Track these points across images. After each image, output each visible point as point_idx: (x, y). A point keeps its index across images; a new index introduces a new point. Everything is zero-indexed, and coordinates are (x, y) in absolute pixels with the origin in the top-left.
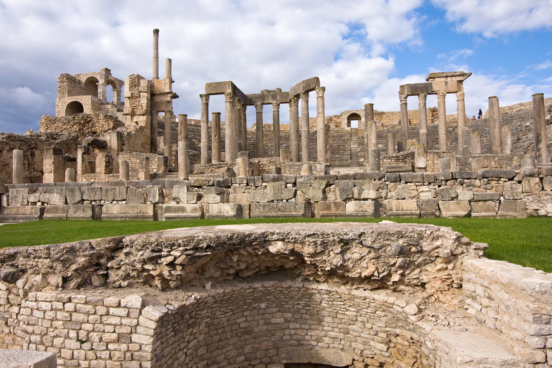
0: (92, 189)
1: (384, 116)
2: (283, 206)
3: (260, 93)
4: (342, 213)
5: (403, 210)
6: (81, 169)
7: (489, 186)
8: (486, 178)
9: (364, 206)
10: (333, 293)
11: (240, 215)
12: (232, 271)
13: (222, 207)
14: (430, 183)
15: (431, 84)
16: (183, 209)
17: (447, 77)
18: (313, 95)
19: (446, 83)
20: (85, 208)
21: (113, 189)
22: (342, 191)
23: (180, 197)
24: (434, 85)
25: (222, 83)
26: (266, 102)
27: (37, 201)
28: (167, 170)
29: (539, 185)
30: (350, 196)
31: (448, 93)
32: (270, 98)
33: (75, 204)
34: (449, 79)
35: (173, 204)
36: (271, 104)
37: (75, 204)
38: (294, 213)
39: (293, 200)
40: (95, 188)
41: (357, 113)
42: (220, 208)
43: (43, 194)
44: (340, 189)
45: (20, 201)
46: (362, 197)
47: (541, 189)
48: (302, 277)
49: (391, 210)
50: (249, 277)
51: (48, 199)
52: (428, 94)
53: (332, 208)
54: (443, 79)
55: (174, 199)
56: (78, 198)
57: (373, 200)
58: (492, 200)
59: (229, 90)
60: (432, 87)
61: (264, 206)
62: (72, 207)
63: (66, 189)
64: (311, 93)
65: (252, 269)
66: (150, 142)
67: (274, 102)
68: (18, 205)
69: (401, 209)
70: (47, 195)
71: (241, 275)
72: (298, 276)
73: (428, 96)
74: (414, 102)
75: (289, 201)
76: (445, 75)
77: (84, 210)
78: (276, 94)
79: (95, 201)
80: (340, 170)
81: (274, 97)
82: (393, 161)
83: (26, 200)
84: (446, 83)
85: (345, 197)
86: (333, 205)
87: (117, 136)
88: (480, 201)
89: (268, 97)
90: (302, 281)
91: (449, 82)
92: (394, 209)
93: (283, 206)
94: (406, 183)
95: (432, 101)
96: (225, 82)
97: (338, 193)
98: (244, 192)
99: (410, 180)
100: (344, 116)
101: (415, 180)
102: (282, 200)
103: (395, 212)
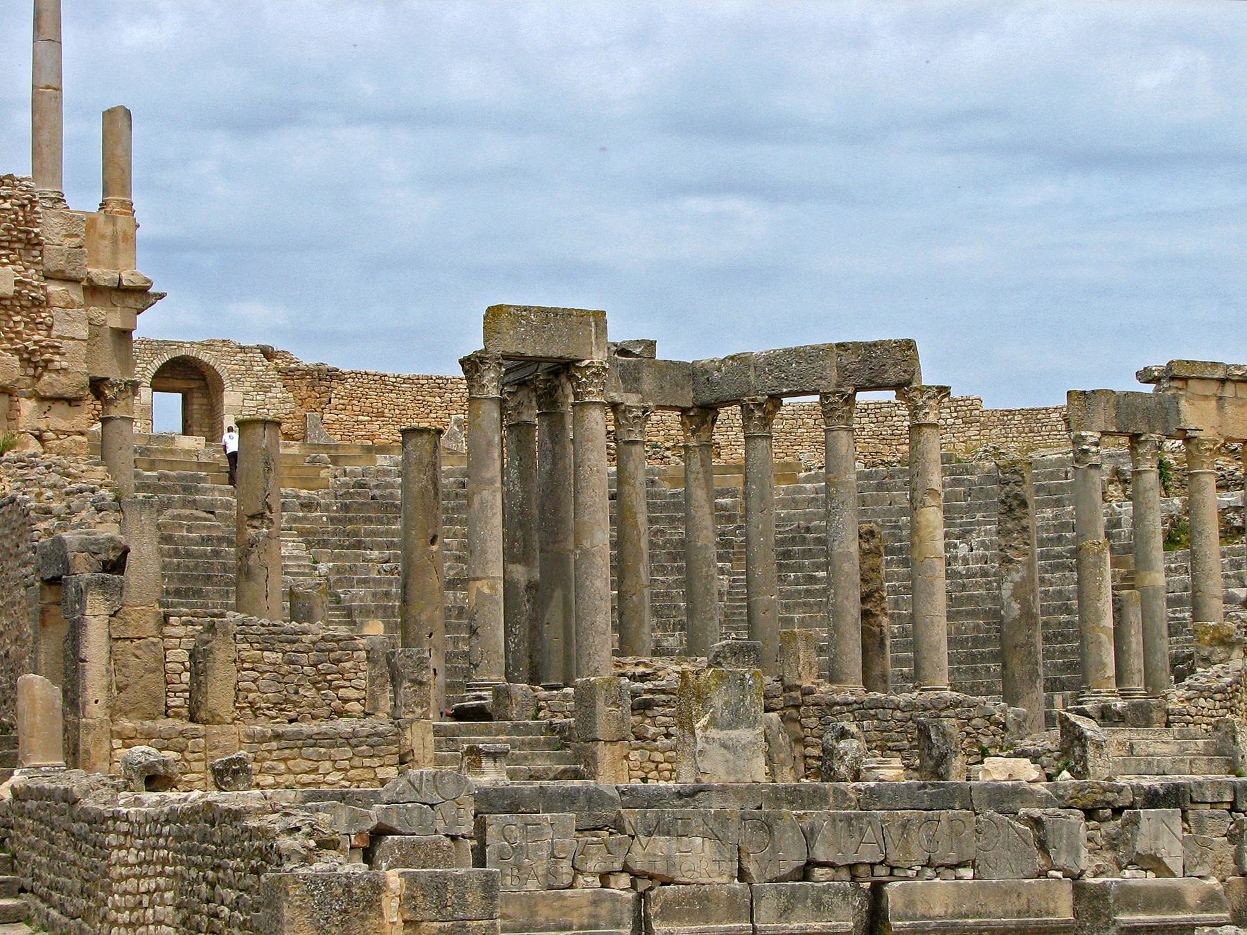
1: (339, 389)
6: (103, 697)
16: (1174, 900)
20: (826, 897)
23: (1162, 853)
27: (618, 866)
41: (205, 357)
43: (644, 839)
45: (540, 871)
51: (668, 858)
60: (1178, 412)
67: (632, 400)
68: (532, 885)
70: (661, 843)
76: (1220, 374)
77: (818, 903)
78: (637, 368)
83: (565, 866)
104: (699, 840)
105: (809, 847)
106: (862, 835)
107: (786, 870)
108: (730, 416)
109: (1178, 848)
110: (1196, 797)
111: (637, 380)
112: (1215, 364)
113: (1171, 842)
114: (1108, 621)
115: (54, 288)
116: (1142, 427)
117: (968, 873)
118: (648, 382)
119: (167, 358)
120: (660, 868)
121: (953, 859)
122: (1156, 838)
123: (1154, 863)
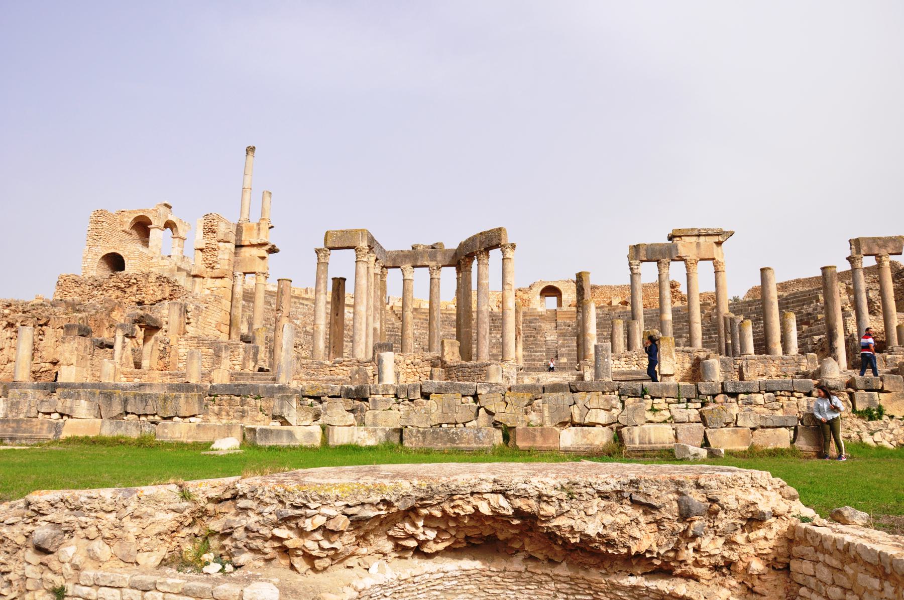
0: (141, 396)
2: (456, 433)
3: (411, 249)
4: (553, 446)
5: (650, 443)
7: (776, 405)
8: (773, 392)
9: (590, 436)
10: (578, 581)
11: (395, 446)
12: (412, 544)
13: (356, 432)
14: (689, 400)
15: (676, 246)
17: (699, 236)
18: (495, 254)
19: (698, 244)
20: (129, 427)
21: (175, 397)
22: (556, 409)
23: (285, 415)
24: (680, 247)
25: (352, 231)
26: (419, 264)
28: (257, 368)
29: (848, 405)
30: (567, 419)
31: (701, 260)
32: (426, 256)
33: (115, 418)
34: (702, 239)
35: (276, 425)
36: (427, 266)
37: (115, 418)
38: (475, 445)
39: (474, 423)
40: (145, 395)
41: (555, 285)
42: (353, 435)
44: (550, 408)
46: (587, 421)
47: (850, 410)
48: (524, 553)
49: (632, 441)
50: (437, 553)
51: (71, 408)
52: (673, 260)
53: (538, 439)
54: (694, 239)
55: (274, 418)
56: (117, 409)
57: (604, 426)
58: (786, 427)
59: (363, 244)
61: (424, 433)
62: (107, 422)
63: (100, 393)
64: (491, 252)
65: (443, 541)
66: (228, 323)
68: (22, 416)
69: (647, 440)
70: (69, 402)
71: (426, 550)
72: (517, 551)
73: (672, 263)
74: (648, 272)
75: (467, 425)
76: (696, 233)
78: (435, 253)
79: (146, 415)
80: (540, 376)
81: (433, 257)
82: (623, 363)
84: (698, 244)
86: (538, 434)
87: (180, 310)
88: (768, 427)
89: (422, 257)
90: (525, 560)
91: (702, 244)
92: (637, 441)
93: (456, 433)
94: (653, 398)
95: (676, 271)
96: (356, 231)
97: (546, 413)
98: (390, 409)
99: (658, 394)
100: (534, 289)
101: (665, 395)
102: (456, 423)
103: (637, 445)
104: (83, 402)
105: (125, 407)
106: (147, 402)
107: (115, 414)
109: (294, 412)
110: (372, 392)
111: (435, 257)
112: (692, 230)
113: (289, 410)
115: (221, 244)
116: (659, 257)
118: (439, 258)
119: (544, 286)
122: (281, 407)
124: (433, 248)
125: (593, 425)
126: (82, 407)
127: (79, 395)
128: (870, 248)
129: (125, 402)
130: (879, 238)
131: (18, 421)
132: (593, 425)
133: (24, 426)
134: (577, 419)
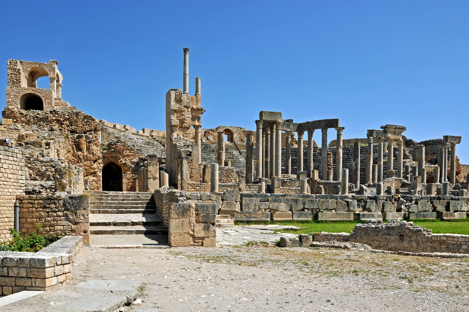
41: (231, 129)
51: (277, 206)
56: (301, 207)
68: (251, 211)
70: (276, 204)
81: (288, 126)
83: (257, 207)
85: (454, 210)
96: (277, 113)
108: (306, 133)
114: (371, 170)
117: (334, 211)
120: (275, 208)
121: (332, 208)
123: (369, 210)
124: (287, 121)
125: (463, 211)
126: (283, 207)
127: (281, 200)
128: (451, 140)
129: (304, 204)
130: (454, 137)
131: (250, 213)
132: (463, 211)
133: (253, 215)
134: (459, 210)
